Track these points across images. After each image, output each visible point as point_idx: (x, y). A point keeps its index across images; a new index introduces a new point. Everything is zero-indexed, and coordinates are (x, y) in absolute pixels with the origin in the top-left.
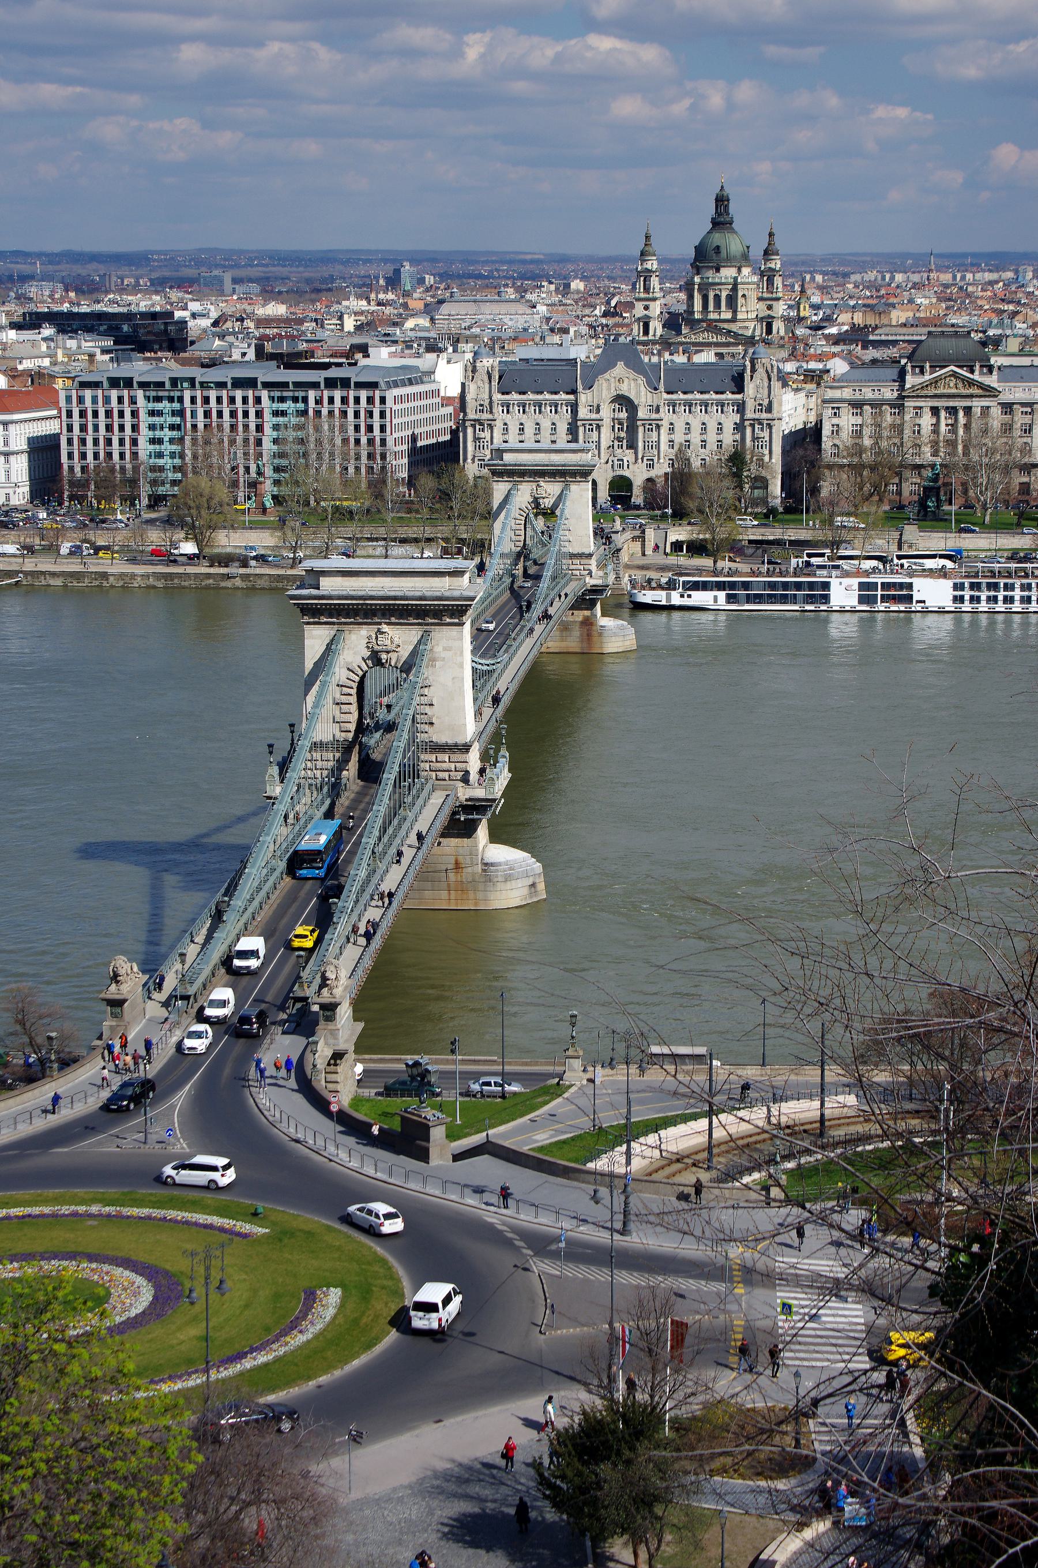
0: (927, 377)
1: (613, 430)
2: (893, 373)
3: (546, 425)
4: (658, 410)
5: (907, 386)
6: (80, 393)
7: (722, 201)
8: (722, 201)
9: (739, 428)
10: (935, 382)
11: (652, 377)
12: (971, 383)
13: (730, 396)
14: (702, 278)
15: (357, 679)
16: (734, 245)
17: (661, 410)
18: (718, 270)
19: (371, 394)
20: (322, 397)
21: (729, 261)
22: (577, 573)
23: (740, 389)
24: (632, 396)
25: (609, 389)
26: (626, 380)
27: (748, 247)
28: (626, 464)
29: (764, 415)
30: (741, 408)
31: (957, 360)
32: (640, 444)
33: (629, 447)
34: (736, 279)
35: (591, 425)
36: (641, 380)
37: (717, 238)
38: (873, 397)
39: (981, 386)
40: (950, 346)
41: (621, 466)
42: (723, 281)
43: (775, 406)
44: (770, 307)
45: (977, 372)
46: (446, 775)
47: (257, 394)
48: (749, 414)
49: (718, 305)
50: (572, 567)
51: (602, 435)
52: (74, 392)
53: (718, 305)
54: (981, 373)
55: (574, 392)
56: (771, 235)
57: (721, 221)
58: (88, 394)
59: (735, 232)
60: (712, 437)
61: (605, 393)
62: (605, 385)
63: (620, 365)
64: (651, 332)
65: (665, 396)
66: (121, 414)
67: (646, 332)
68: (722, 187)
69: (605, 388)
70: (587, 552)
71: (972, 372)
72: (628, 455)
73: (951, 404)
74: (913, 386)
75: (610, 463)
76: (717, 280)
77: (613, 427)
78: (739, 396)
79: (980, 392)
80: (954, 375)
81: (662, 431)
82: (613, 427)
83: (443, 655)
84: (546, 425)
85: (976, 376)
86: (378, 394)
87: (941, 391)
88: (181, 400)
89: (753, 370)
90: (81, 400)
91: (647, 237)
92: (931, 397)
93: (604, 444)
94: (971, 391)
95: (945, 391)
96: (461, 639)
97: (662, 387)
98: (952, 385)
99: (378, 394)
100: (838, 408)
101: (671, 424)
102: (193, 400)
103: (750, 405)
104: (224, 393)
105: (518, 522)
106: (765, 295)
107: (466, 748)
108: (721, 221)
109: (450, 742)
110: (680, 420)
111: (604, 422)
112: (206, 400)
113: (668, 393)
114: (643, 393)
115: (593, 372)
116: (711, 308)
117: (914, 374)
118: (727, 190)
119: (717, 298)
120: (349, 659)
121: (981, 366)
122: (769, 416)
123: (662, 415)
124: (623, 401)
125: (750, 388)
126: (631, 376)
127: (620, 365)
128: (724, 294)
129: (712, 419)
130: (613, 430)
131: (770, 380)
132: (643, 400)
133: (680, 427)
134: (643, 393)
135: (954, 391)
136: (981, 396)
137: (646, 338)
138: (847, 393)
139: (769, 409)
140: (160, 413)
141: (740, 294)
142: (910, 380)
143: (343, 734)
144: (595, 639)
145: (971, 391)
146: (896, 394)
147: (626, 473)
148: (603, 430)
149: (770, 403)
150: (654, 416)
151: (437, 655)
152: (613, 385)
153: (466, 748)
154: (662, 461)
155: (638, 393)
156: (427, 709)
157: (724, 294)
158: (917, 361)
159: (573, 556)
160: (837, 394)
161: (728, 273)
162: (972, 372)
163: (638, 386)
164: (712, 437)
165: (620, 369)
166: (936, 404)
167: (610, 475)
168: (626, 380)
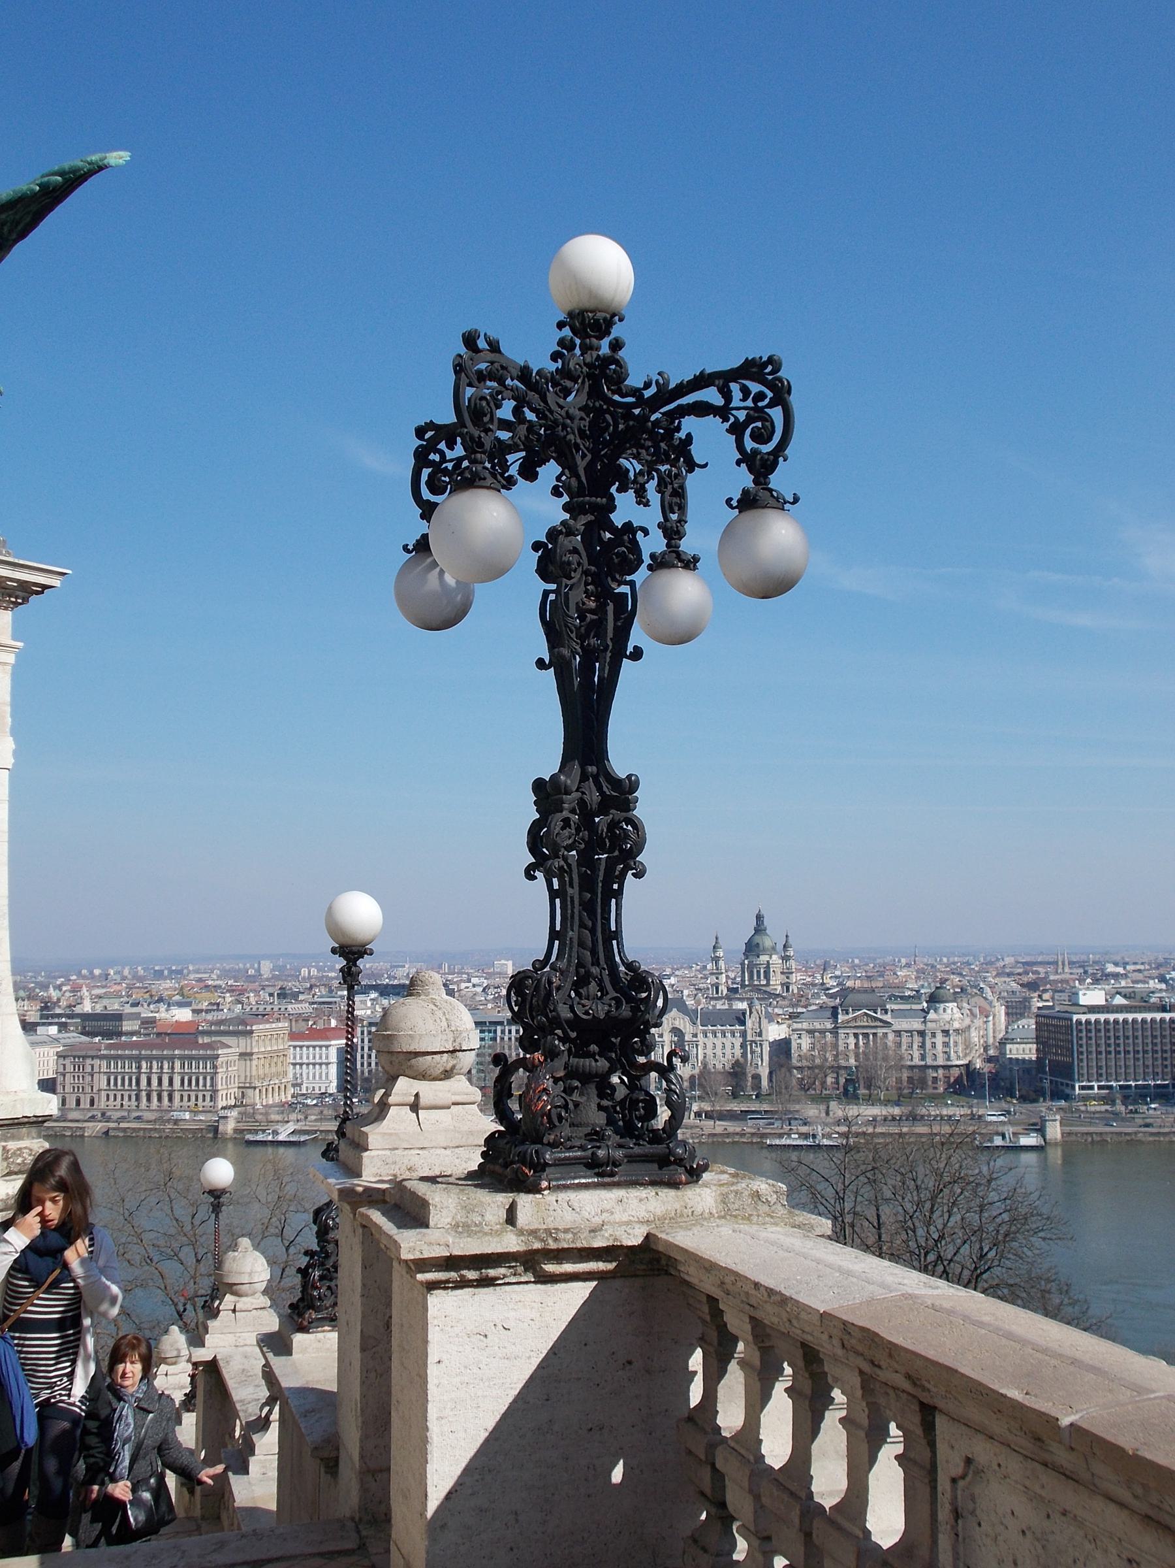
0: (851, 1016)
7: (759, 918)
8: (759, 918)
10: (855, 1019)
11: (692, 1015)
12: (876, 1019)
13: (738, 1027)
21: (765, 951)
23: (743, 1023)
29: (758, 1038)
30: (744, 1034)
37: (757, 939)
39: (881, 1021)
44: (788, 978)
48: (749, 1038)
54: (881, 1014)
56: (787, 936)
57: (759, 929)
60: (728, 1051)
65: (700, 1027)
73: (865, 1031)
79: (881, 1024)
85: (879, 1015)
89: (751, 1013)
103: (749, 1032)
108: (759, 929)
118: (762, 912)
119: (759, 972)
123: (699, 1038)
124: (676, 1031)
125: (749, 1023)
128: (762, 971)
133: (710, 1046)
135: (866, 1024)
138: (805, 1026)
142: (841, 1018)
149: (761, 1031)
157: (762, 971)
160: (799, 1026)
161: (764, 958)
164: (728, 1051)
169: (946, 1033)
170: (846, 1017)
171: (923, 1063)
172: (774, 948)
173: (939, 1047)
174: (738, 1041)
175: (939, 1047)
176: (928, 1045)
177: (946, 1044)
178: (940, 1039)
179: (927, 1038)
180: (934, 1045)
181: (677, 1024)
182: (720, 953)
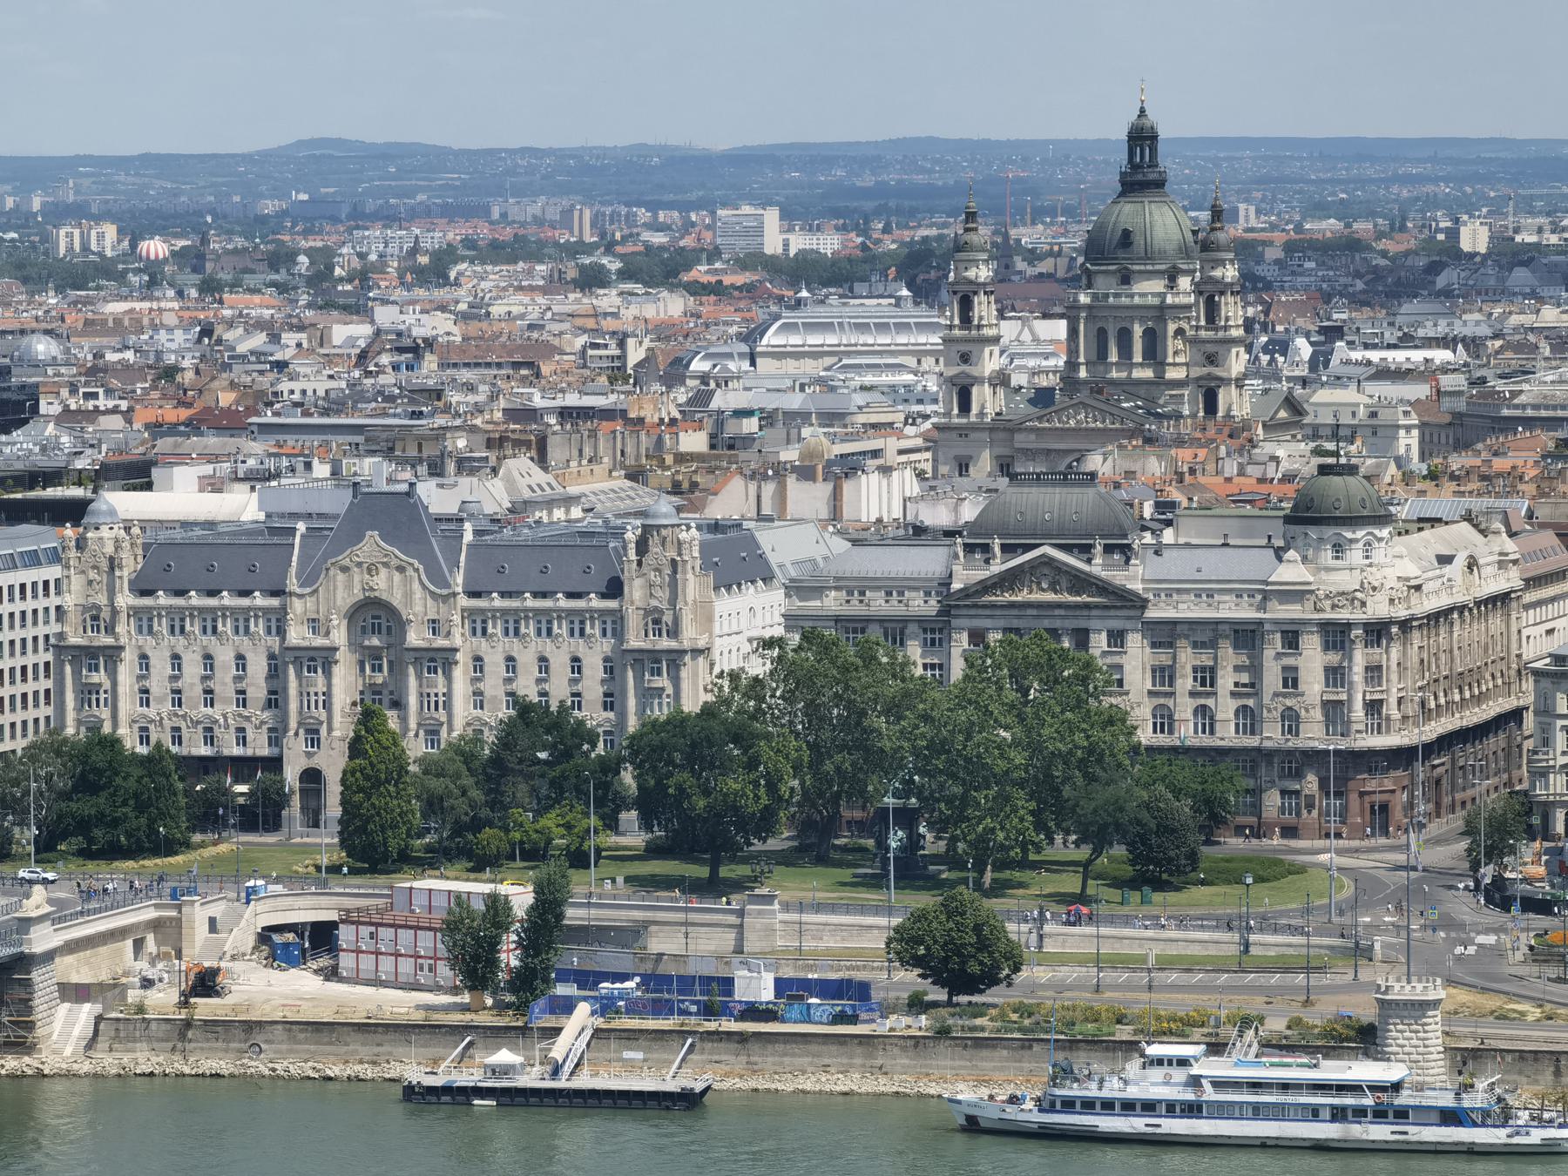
0: (997, 567)
1: (362, 670)
3: (225, 656)
10: (1009, 580)
12: (1081, 582)
13: (596, 603)
14: (1095, 297)
18: (1126, 279)
24: (396, 600)
25: (349, 586)
30: (615, 625)
32: (412, 700)
34: (1162, 296)
35: (312, 659)
39: (1103, 588)
42: (1137, 300)
45: (1098, 560)
51: (336, 681)
55: (277, 593)
61: (340, 593)
62: (341, 577)
63: (373, 536)
64: (975, 409)
67: (965, 407)
68: (1142, 111)
71: (1089, 561)
78: (612, 604)
80: (1048, 561)
84: (225, 656)
85: (1097, 567)
87: (1022, 596)
92: (1002, 606)
94: (1085, 598)
103: (634, 621)
116: (1113, 357)
118: (1153, 116)
119: (1125, 337)
127: (373, 536)
130: (362, 670)
132: (418, 608)
136: (1106, 607)
137: (964, 421)
145: (1085, 598)
152: (357, 578)
155: (408, 595)
157: (1138, 330)
161: (1148, 289)
162: (1089, 561)
163: (407, 582)
165: (372, 544)
169: (1336, 635)
170: (982, 574)
171: (1252, 742)
173: (1314, 686)
175: (1314, 686)
176: (1272, 679)
177: (1335, 675)
178: (1313, 658)
179: (1269, 654)
180: (1291, 679)
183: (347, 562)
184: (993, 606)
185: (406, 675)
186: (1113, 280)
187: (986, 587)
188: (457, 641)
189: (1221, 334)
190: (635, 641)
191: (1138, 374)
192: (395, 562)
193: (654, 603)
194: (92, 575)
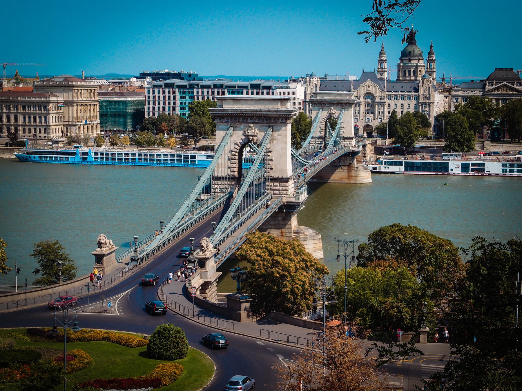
0: (495, 86)
1: (366, 106)
2: (481, 85)
4: (384, 99)
5: (486, 90)
6: (153, 90)
9: (416, 106)
10: (497, 89)
13: (413, 93)
14: (404, 64)
15: (239, 148)
16: (416, 51)
17: (385, 98)
18: (410, 61)
19: (268, 91)
20: (248, 92)
22: (347, 145)
23: (417, 90)
24: (373, 93)
25: (364, 90)
26: (371, 87)
27: (422, 52)
28: (370, 120)
29: (427, 101)
30: (417, 98)
31: (507, 80)
32: (376, 112)
33: (372, 113)
34: (417, 64)
36: (377, 87)
37: (410, 49)
38: (472, 94)
39: (517, 90)
40: (504, 75)
41: (368, 121)
42: (412, 65)
43: (432, 97)
45: (515, 85)
46: (277, 192)
47: (223, 90)
48: (421, 101)
49: (410, 74)
50: (344, 143)
51: (361, 108)
52: (151, 89)
53: (410, 74)
54: (517, 86)
58: (156, 90)
59: (417, 47)
61: (362, 91)
62: (362, 88)
63: (369, 80)
65: (387, 93)
66: (169, 98)
69: (362, 91)
70: (351, 137)
71: (513, 85)
72: (371, 117)
74: (489, 90)
75: (364, 120)
76: (410, 65)
77: (365, 105)
78: (417, 94)
80: (505, 85)
81: (385, 107)
82: (365, 105)
83: (277, 138)
85: (515, 86)
86: (271, 91)
87: (500, 92)
88: (193, 92)
89: (423, 83)
90: (154, 92)
91: (383, 47)
93: (362, 112)
94: (513, 92)
95: (502, 92)
96: (286, 130)
97: (386, 89)
98: (505, 89)
99: (271, 91)
100: (458, 99)
101: (389, 104)
102: (198, 93)
103: (421, 97)
104: (210, 90)
105: (322, 124)
106: (428, 70)
107: (287, 180)
109: (280, 177)
110: (393, 103)
111: (362, 103)
112: (203, 93)
113: (388, 92)
114: (378, 92)
115: (358, 83)
116: (407, 76)
117: (489, 85)
119: (410, 71)
120: (235, 139)
121: (517, 83)
122: (429, 101)
123: (385, 100)
124: (369, 95)
125: (421, 91)
126: (373, 85)
127: (369, 80)
128: (412, 70)
129: (406, 103)
130: (366, 106)
131: (429, 87)
132: (378, 94)
134: (378, 92)
138: (461, 93)
139: (429, 99)
140: (184, 98)
141: (419, 70)
142: (488, 88)
143: (232, 173)
144: (353, 173)
145: (513, 92)
146: (481, 93)
147: (371, 124)
148: (361, 106)
149: (430, 96)
150: (382, 101)
151: (275, 138)
152: (366, 88)
153: (287, 180)
154: (385, 119)
155: (376, 92)
156: (270, 162)
157: (412, 70)
158: (490, 80)
159: (345, 138)
161: (414, 62)
162: (513, 85)
163: (376, 89)
165: (369, 82)
166: (498, 98)
167: (364, 124)
168: (371, 87)
170: (492, 88)
172: (421, 55)
174: (413, 103)
181: (370, 89)
182: (384, 58)
183: (364, 85)
184: (494, 94)
185: (375, 107)
186: (407, 61)
187: (492, 90)
188: (385, 100)
189: (432, 70)
190: (421, 101)
191: (412, 79)
192: (373, 85)
193: (425, 93)
194: (312, 87)
